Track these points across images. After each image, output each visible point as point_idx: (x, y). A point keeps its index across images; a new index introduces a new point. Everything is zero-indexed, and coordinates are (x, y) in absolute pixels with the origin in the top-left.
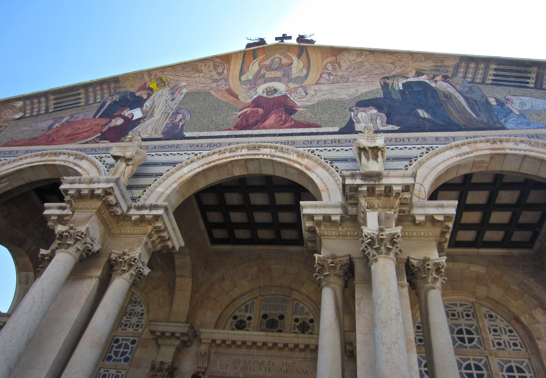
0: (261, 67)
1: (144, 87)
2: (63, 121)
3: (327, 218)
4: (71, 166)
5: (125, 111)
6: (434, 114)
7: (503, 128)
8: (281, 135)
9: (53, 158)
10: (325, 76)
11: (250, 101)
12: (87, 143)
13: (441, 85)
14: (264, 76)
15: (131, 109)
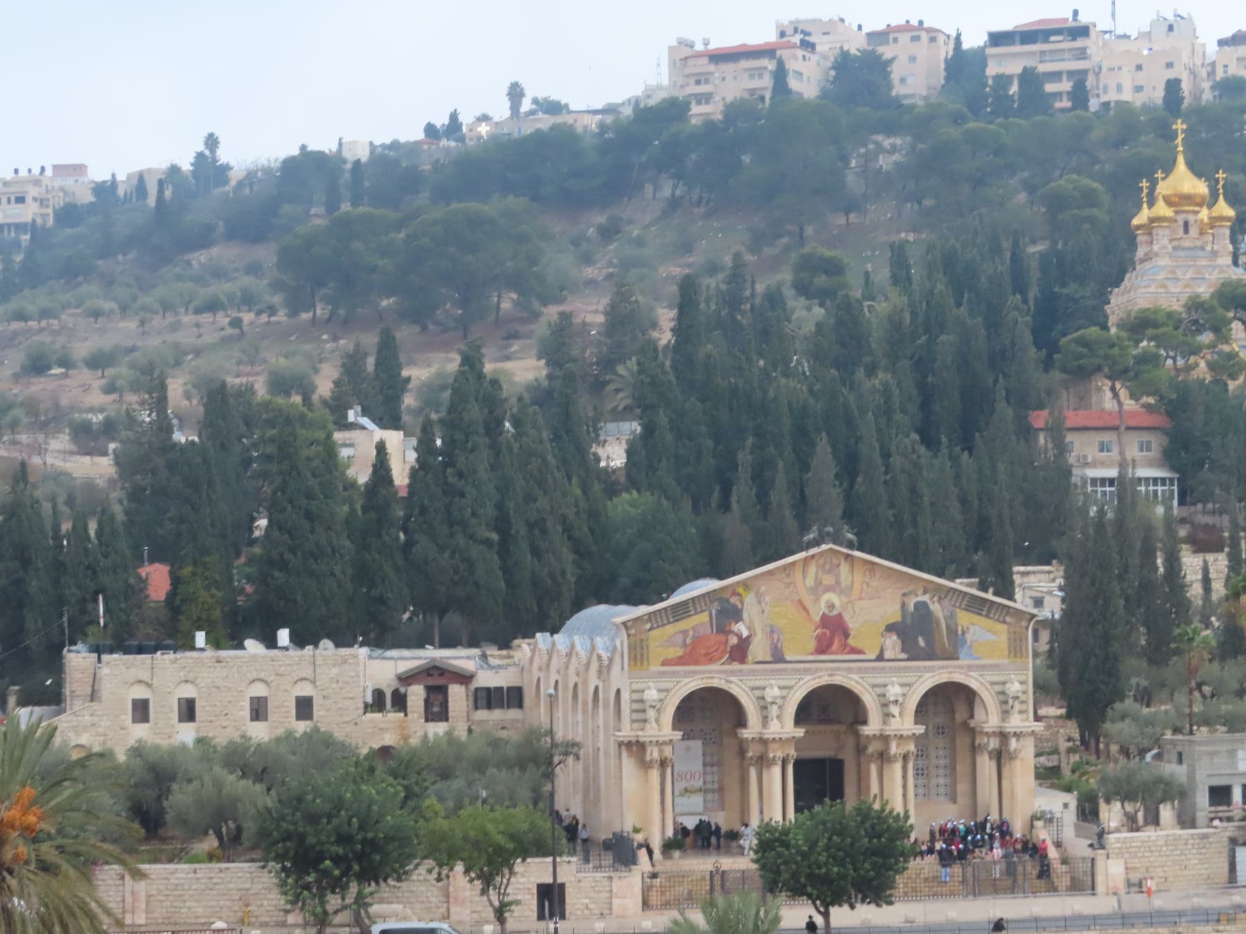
0: (818, 567)
1: (735, 593)
2: (690, 636)
3: (874, 735)
4: (726, 688)
5: (733, 625)
6: (927, 642)
7: (957, 659)
8: (844, 661)
9: (710, 681)
10: (865, 586)
11: (818, 619)
12: (723, 664)
13: (935, 608)
14: (821, 582)
15: (737, 622)
